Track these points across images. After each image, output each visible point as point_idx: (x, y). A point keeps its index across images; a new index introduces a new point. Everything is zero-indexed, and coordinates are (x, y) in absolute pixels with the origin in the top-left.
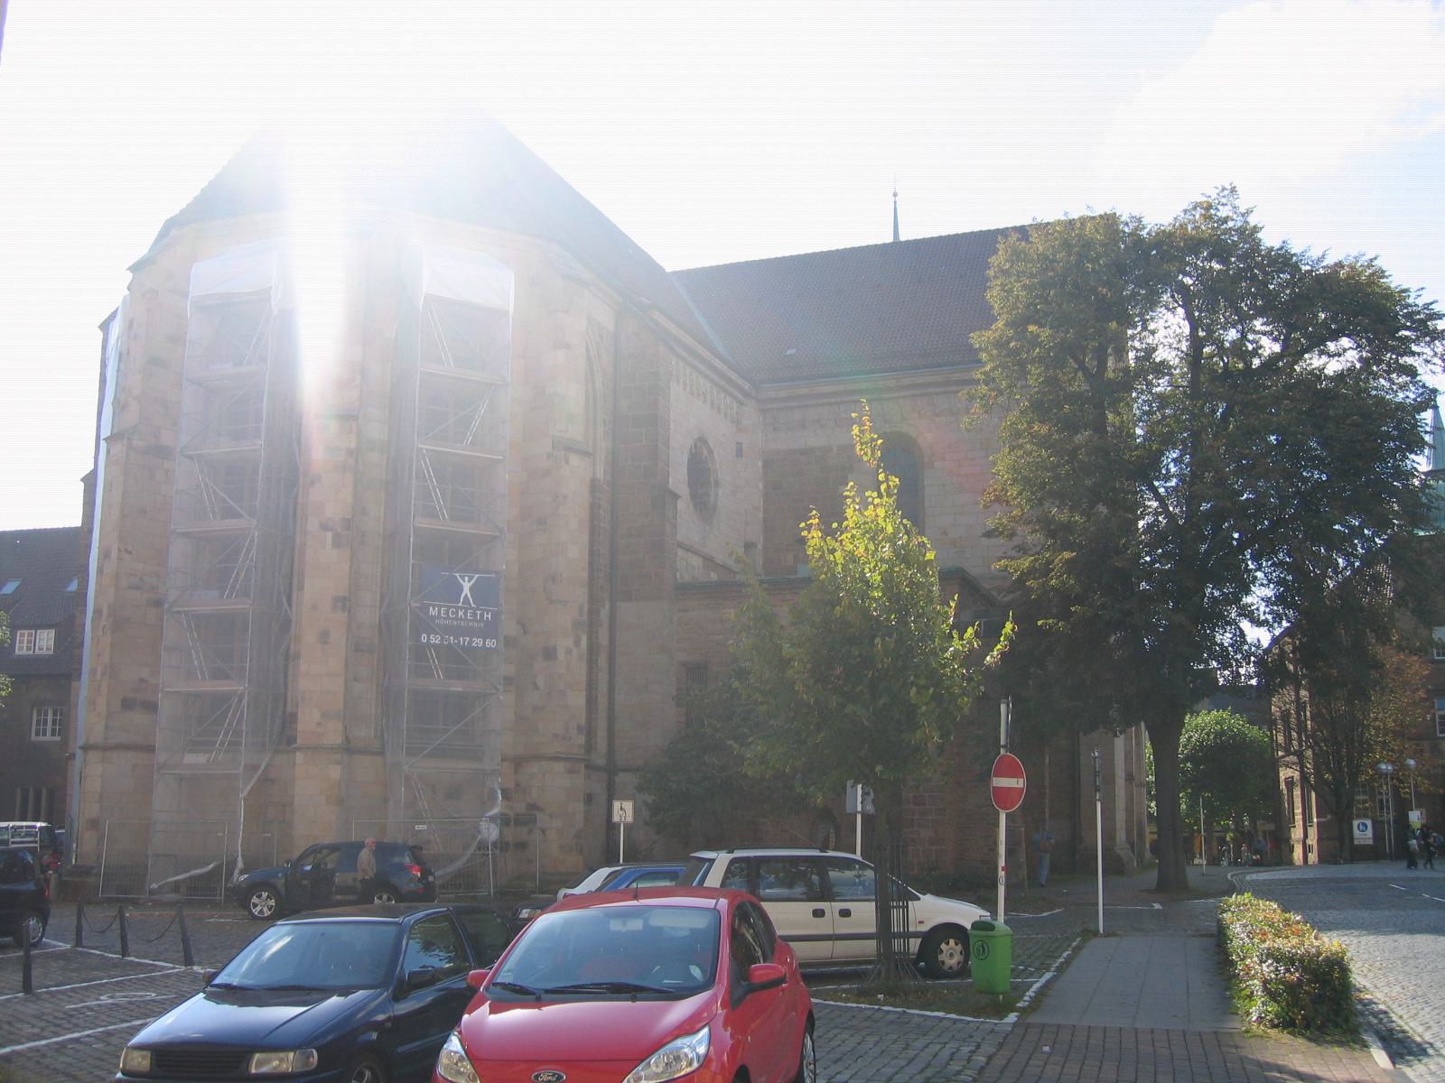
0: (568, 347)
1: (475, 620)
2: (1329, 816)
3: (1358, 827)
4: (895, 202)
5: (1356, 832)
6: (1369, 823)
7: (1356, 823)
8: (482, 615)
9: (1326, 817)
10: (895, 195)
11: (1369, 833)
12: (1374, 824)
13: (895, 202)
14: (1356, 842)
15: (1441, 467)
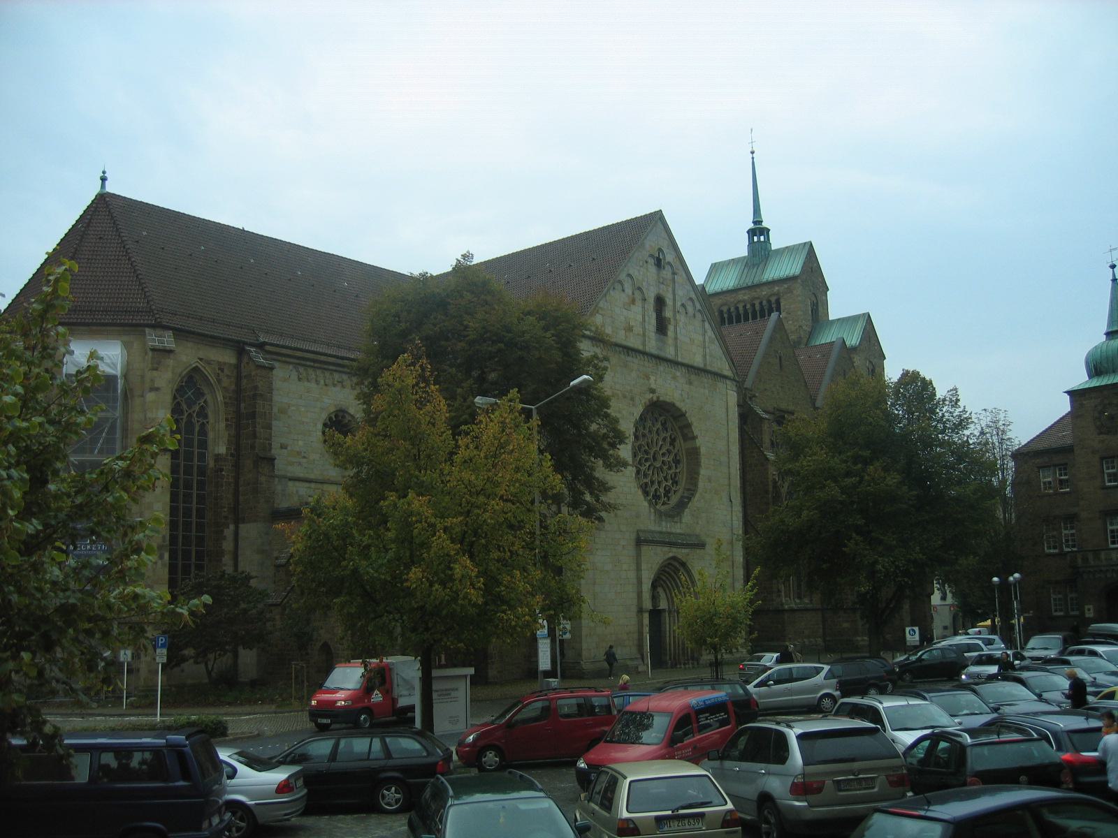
0: (157, 389)
1: (97, 550)
2: (1031, 612)
3: (909, 632)
4: (753, 158)
5: (908, 636)
6: (916, 629)
7: (907, 629)
8: (101, 547)
9: (1029, 613)
10: (752, 153)
11: (917, 637)
13: (753, 158)
14: (908, 644)
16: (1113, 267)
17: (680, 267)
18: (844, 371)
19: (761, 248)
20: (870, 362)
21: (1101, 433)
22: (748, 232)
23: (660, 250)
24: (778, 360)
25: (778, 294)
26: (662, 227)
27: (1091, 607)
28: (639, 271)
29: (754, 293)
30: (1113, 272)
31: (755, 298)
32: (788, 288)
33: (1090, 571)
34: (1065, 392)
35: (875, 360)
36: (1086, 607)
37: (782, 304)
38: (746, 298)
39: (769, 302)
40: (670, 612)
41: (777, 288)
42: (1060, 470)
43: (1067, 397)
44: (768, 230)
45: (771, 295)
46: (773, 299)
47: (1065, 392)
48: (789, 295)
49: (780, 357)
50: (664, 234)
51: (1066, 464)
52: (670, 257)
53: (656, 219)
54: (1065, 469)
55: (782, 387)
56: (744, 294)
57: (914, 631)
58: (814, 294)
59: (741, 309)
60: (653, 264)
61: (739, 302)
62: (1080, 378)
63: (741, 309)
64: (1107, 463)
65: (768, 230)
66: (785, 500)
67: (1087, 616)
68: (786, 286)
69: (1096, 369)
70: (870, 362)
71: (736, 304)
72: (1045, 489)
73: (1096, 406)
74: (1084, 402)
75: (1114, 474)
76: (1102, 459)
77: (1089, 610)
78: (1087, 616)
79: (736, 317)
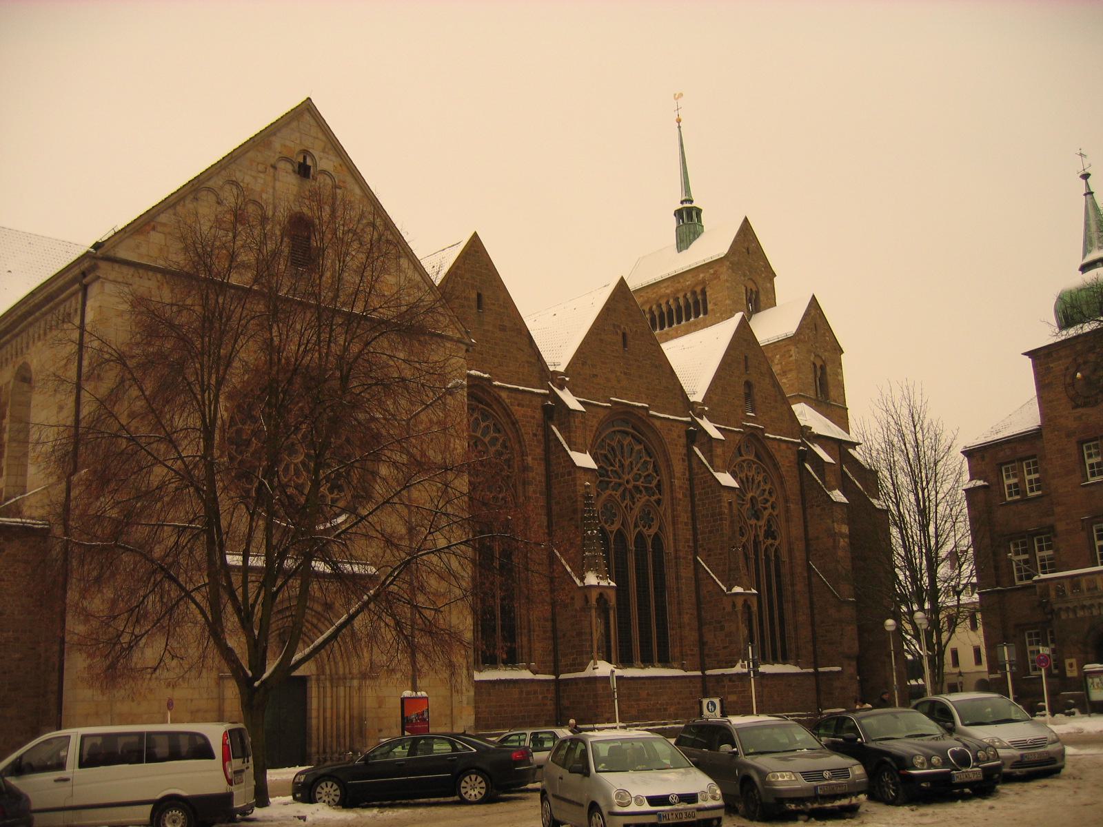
4: (679, 127)
6: (717, 701)
7: (705, 702)
12: (721, 701)
13: (679, 127)
15: (1095, 255)
16: (1086, 176)
17: (349, 179)
18: (746, 357)
19: (689, 232)
20: (817, 356)
21: (1076, 406)
22: (675, 215)
23: (306, 153)
24: (620, 338)
25: (703, 281)
26: (315, 124)
27: (1073, 661)
28: (255, 178)
29: (678, 285)
30: (1087, 184)
31: (678, 291)
32: (714, 274)
33: (1068, 608)
34: (1025, 354)
35: (826, 354)
36: (1068, 662)
37: (708, 294)
38: (668, 291)
39: (694, 293)
40: (318, 680)
41: (701, 275)
42: (1028, 465)
43: (1028, 361)
44: (699, 211)
45: (697, 285)
46: (698, 289)
47: (1025, 354)
48: (715, 282)
49: (624, 335)
50: (315, 131)
51: (1034, 456)
52: (326, 163)
53: (307, 110)
54: (1035, 463)
55: (625, 374)
56: (667, 288)
57: (713, 704)
58: (751, 279)
59: (664, 308)
60: (290, 171)
61: (661, 297)
62: (1047, 333)
63: (664, 308)
64: (1089, 448)
65: (699, 211)
66: (636, 526)
67: (1069, 674)
68: (712, 271)
69: (1066, 317)
70: (817, 356)
71: (658, 301)
72: (1010, 495)
73: (1067, 369)
74: (1051, 365)
75: (1099, 464)
76: (1080, 443)
77: (1071, 665)
78: (1069, 674)
79: (659, 317)
